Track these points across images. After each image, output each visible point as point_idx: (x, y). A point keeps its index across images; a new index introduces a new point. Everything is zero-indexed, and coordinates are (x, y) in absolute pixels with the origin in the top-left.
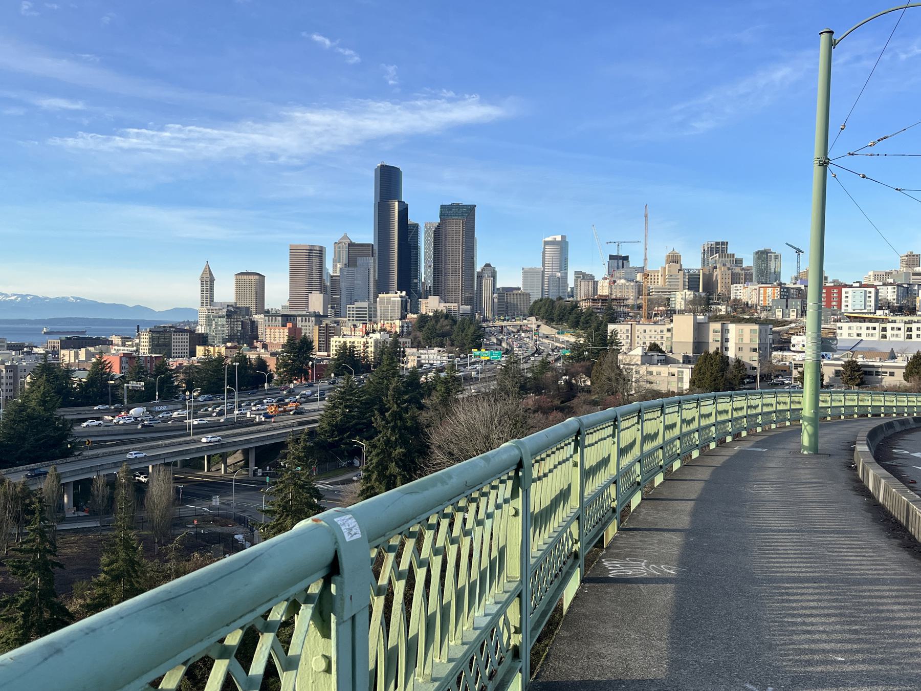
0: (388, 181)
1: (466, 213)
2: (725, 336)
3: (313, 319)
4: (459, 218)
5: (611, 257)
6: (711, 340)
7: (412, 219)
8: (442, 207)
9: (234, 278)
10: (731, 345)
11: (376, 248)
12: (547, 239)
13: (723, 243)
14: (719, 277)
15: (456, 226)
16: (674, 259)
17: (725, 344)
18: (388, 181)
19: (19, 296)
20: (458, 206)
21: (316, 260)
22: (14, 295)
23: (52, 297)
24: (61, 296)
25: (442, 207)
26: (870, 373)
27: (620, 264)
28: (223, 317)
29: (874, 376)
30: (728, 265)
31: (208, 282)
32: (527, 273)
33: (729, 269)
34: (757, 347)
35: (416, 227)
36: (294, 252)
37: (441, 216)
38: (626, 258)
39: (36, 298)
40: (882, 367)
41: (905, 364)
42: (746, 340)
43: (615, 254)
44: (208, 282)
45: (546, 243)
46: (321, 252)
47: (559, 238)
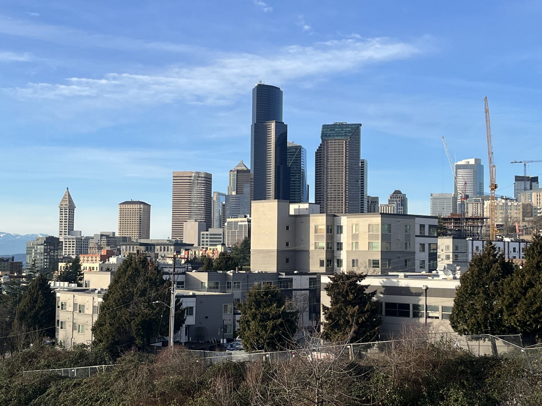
0: (268, 101)
2: (336, 241)
3: (172, 247)
4: (343, 137)
5: (518, 179)
6: (312, 248)
7: (292, 140)
9: (118, 207)
10: (343, 255)
11: (252, 172)
12: (459, 163)
15: (340, 146)
17: (336, 253)
18: (268, 101)
24: (30, 234)
27: (528, 186)
28: (41, 245)
29: (410, 320)
31: (69, 210)
32: (436, 200)
34: (378, 257)
36: (178, 179)
37: (324, 136)
38: (535, 180)
39: (8, 235)
40: (427, 291)
42: (363, 246)
44: (69, 210)
45: (458, 167)
46: (208, 179)
47: (472, 162)
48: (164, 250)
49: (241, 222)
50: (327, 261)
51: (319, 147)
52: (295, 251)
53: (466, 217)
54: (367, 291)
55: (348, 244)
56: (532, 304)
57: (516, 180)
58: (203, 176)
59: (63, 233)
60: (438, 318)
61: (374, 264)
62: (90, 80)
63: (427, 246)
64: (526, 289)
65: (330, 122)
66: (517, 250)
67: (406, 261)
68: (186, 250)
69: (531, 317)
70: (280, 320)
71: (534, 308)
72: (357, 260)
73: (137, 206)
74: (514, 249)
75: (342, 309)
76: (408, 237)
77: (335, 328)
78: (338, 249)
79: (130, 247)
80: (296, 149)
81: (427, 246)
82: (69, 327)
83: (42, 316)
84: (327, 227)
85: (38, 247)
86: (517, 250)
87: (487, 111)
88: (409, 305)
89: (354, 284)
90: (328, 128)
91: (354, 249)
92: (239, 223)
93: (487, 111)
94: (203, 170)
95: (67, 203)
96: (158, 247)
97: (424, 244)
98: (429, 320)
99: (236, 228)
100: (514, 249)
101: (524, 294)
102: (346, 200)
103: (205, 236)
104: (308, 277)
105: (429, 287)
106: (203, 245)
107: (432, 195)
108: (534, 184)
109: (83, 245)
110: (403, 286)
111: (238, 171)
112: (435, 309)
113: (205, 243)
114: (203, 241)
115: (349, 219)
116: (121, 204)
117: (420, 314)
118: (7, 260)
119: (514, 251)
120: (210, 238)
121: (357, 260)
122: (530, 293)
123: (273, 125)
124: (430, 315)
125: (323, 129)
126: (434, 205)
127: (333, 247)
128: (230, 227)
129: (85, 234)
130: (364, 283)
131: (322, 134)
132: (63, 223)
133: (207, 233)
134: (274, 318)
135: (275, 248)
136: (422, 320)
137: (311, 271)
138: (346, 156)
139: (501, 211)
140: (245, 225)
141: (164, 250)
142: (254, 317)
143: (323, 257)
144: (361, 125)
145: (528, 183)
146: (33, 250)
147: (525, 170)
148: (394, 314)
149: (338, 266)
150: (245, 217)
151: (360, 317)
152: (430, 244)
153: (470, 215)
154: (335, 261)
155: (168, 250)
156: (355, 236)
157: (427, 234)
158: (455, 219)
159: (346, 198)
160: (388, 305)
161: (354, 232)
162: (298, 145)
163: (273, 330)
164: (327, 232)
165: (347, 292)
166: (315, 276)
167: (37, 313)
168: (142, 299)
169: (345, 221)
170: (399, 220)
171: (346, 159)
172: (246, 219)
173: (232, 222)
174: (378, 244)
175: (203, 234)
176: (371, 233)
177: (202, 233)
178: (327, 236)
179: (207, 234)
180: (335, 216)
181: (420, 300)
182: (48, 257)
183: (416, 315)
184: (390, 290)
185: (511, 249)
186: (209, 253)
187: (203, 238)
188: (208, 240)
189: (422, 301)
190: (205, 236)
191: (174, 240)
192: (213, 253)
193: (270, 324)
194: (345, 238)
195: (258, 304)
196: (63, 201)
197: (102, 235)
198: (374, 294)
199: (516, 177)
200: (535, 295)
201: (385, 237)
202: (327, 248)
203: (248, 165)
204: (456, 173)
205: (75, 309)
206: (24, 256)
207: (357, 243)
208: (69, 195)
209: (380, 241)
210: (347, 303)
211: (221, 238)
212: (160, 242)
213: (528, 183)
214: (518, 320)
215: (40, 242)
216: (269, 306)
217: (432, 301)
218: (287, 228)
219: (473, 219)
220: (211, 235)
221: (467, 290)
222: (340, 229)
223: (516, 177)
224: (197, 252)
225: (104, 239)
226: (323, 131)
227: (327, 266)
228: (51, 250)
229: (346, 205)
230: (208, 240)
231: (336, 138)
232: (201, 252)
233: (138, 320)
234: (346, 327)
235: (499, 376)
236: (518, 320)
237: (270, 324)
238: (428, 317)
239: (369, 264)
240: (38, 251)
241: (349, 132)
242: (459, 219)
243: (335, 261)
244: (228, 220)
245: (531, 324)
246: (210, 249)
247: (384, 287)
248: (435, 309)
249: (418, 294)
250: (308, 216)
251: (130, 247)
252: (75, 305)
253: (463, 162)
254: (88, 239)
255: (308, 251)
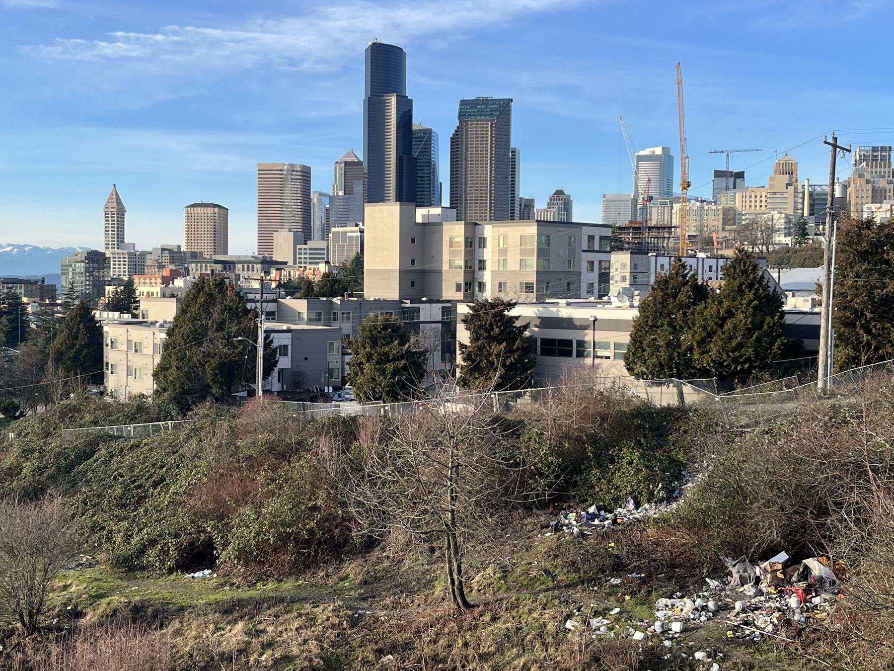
0: (386, 66)
1: (500, 111)
2: (478, 257)
3: (259, 266)
5: (718, 174)
6: (445, 267)
7: (418, 122)
8: (463, 103)
10: (487, 277)
11: (365, 165)
12: (642, 153)
13: (883, 149)
14: (853, 195)
16: (788, 170)
17: (478, 274)
18: (386, 66)
19: (15, 246)
20: (486, 102)
21: (298, 186)
22: (10, 245)
23: (55, 247)
24: (66, 246)
25: (463, 103)
26: (563, 348)
27: (731, 185)
28: (81, 262)
29: (574, 360)
30: (868, 176)
31: (117, 215)
32: (610, 203)
33: (868, 182)
34: (533, 279)
35: (427, 134)
37: (462, 115)
38: (740, 175)
39: (35, 249)
41: (632, 314)
42: (513, 264)
43: (723, 168)
44: (117, 215)
45: (641, 158)
46: (306, 174)
47: (658, 151)
48: (248, 270)
49: (351, 232)
50: (466, 284)
51: (456, 131)
52: (423, 272)
53: (649, 225)
54: (517, 324)
55: (493, 262)
56: (730, 338)
57: (715, 176)
58: (299, 169)
59: (110, 246)
60: (609, 358)
61: (526, 287)
62: (142, 35)
63: (596, 264)
64: (724, 319)
65: (472, 97)
66: (714, 269)
67: (569, 284)
68: (277, 269)
69: (728, 356)
70: (403, 362)
71: (734, 343)
72: (505, 283)
73: (210, 210)
74: (711, 267)
75: (484, 347)
76: (572, 253)
77: (475, 371)
78: (480, 269)
79: (201, 266)
80: (425, 134)
81: (596, 264)
82: (121, 371)
83: (85, 357)
84: (466, 238)
85: (78, 265)
86: (714, 269)
87: (679, 83)
88: (571, 341)
89: (500, 314)
90: (467, 104)
91: (501, 269)
92: (349, 234)
93: (679, 83)
94: (299, 161)
95: (115, 205)
96: (240, 266)
97: (593, 262)
98: (597, 361)
99: (344, 241)
100: (711, 267)
101: (722, 326)
102: (491, 203)
103: (303, 251)
104: (440, 305)
105: (598, 317)
106: (300, 263)
107: (604, 196)
108: (738, 181)
109: (137, 262)
110: (565, 316)
111: (346, 163)
112: (606, 346)
113: (303, 260)
114: (300, 258)
115: (495, 229)
116: (188, 207)
117: (586, 354)
118: (36, 283)
119: (710, 271)
120: (310, 254)
121: (505, 283)
122: (729, 325)
123: (393, 100)
124: (599, 354)
125: (461, 105)
126: (607, 210)
127: (473, 266)
128: (336, 239)
129: (140, 248)
130: (513, 312)
131: (460, 112)
132: (110, 232)
133: (306, 246)
134: (396, 359)
135: (397, 267)
136: (589, 361)
137: (444, 298)
138: (491, 144)
139: (694, 218)
140: (357, 237)
141: (248, 270)
142: (369, 357)
143: (461, 280)
144: (512, 100)
145: (732, 179)
146: (71, 269)
147: (728, 163)
148: (551, 353)
149: (480, 291)
150: (357, 225)
151: (508, 357)
152: (600, 262)
153: (653, 223)
154: (476, 284)
155: (253, 270)
156: (503, 252)
157: (597, 248)
158: (635, 229)
159: (491, 200)
160: (545, 341)
161: (501, 246)
162: (427, 127)
163: (394, 375)
164: (466, 246)
165: (491, 325)
166: (449, 305)
167: (79, 352)
168: (220, 334)
169: (489, 231)
170: (560, 229)
171: (491, 148)
172: (357, 229)
173: (338, 233)
174: (532, 261)
175: (300, 249)
176: (523, 247)
177: (298, 247)
178: (466, 251)
179: (305, 249)
180: (476, 224)
181: (586, 334)
182: (91, 278)
183: (581, 354)
184: (547, 322)
185: (707, 268)
186: (309, 274)
187: (300, 254)
188: (307, 256)
189: (588, 336)
190: (303, 251)
191: (261, 256)
192: (314, 274)
193: (390, 367)
194: (488, 254)
195: (374, 342)
196: (108, 202)
197: (163, 250)
198: (526, 327)
199: (716, 171)
200: (735, 327)
201: (543, 253)
202: (466, 267)
203: (360, 154)
204: (637, 166)
205: (129, 348)
206: (58, 277)
207: (505, 260)
208: (117, 194)
209: (535, 258)
210: (491, 339)
211: (324, 254)
212: (242, 259)
213: (732, 179)
214: (712, 360)
215: (79, 258)
216: (388, 343)
217: (601, 336)
218: (413, 240)
219: (658, 228)
220: (310, 249)
221: (647, 321)
222: (483, 242)
223: (716, 171)
224: (292, 273)
225: (166, 254)
226: (460, 109)
227: (466, 290)
228: (94, 269)
229: (491, 210)
230: (307, 256)
231: (478, 118)
232: (298, 273)
233: (214, 362)
234: (489, 370)
235: (686, 432)
236: (712, 360)
237: (390, 367)
238: (596, 357)
239: (521, 288)
240: (78, 270)
241: (496, 111)
242: (640, 228)
243: (476, 284)
244: (333, 229)
245: (729, 365)
246: (310, 269)
247: (539, 318)
248: (606, 346)
249: (586, 328)
250: (441, 224)
251: (201, 266)
252: (129, 341)
253: (646, 152)
254: (143, 254)
255: (440, 272)
